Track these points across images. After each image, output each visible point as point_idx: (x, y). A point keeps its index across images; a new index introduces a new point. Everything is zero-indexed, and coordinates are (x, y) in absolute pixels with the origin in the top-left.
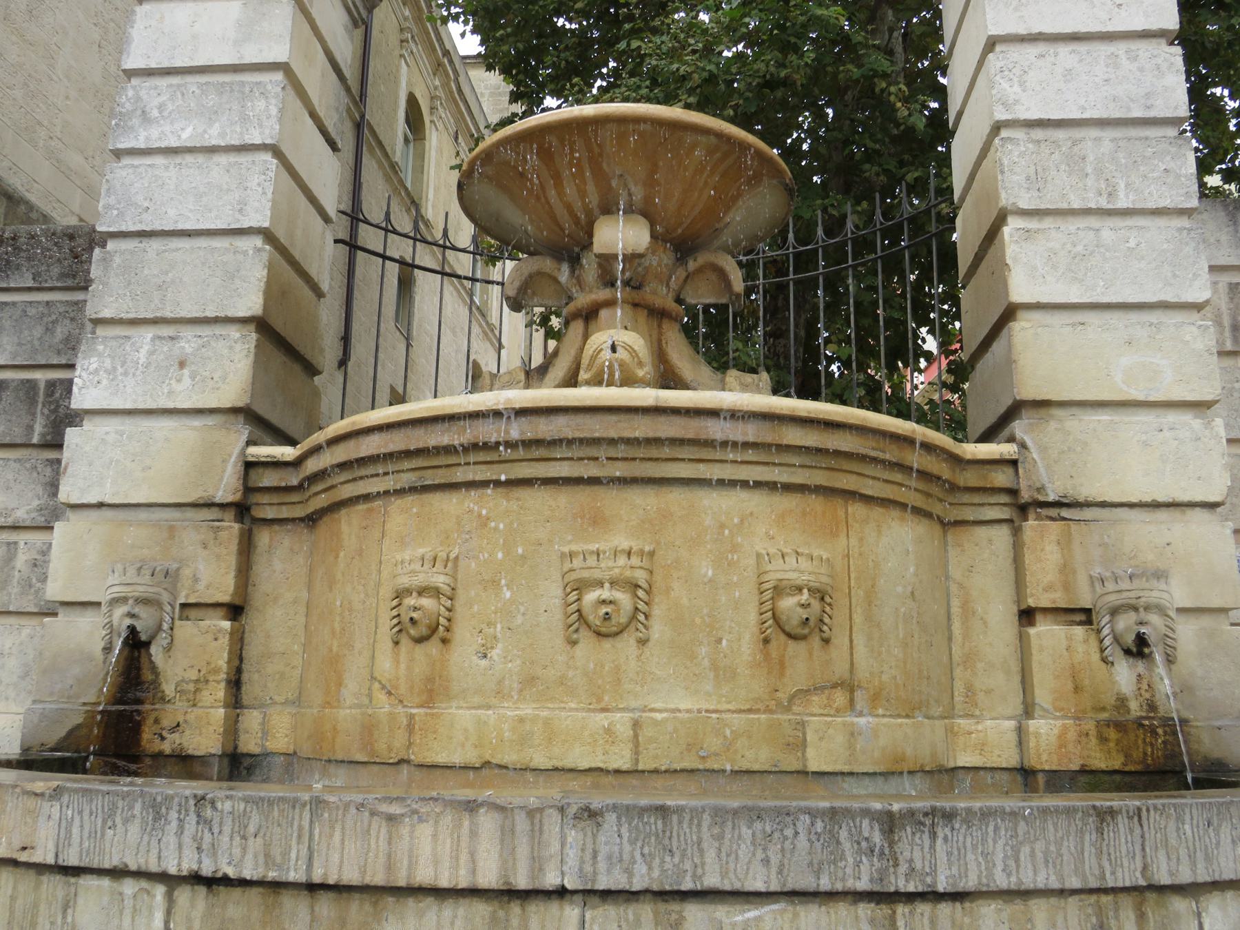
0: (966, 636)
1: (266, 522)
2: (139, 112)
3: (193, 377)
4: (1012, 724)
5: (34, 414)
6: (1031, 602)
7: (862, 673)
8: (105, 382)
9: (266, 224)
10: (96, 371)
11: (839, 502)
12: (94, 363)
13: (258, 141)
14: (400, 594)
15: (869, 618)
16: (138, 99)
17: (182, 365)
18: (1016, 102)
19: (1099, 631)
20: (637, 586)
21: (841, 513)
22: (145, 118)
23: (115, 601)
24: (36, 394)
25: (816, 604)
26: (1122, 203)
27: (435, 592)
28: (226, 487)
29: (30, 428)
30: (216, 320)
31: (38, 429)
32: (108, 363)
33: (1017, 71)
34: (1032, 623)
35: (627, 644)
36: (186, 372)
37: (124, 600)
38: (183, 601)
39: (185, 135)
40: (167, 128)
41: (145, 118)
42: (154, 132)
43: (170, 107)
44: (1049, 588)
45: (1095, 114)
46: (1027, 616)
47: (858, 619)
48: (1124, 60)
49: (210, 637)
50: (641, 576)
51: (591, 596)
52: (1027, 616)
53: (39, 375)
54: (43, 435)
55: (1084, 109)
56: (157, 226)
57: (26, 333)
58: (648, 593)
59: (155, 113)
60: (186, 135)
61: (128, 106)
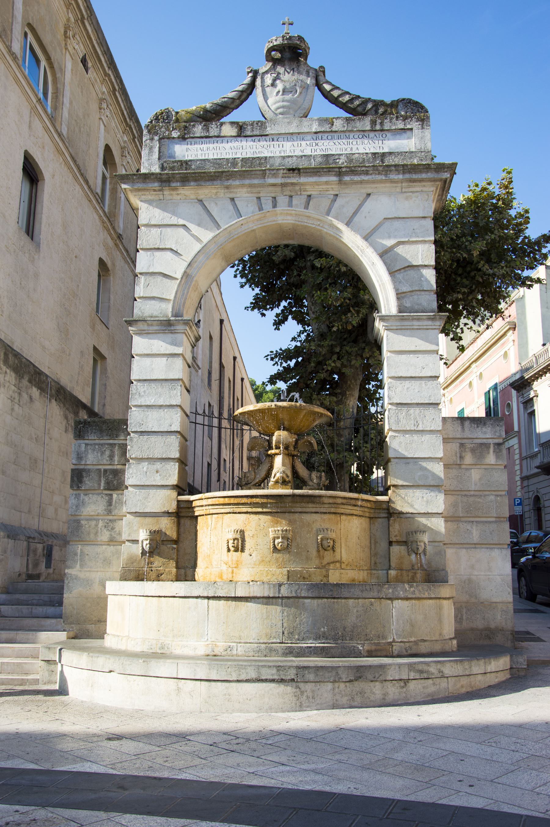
0: (375, 548)
1: (183, 517)
2: (138, 393)
4: (385, 572)
5: (100, 480)
6: (391, 540)
7: (344, 559)
8: (134, 477)
9: (179, 430)
10: (132, 474)
11: (339, 516)
13: (175, 404)
15: (346, 545)
17: (157, 472)
18: (393, 397)
19: (408, 547)
20: (288, 538)
21: (339, 518)
24: (101, 474)
25: (332, 542)
26: (420, 428)
28: (172, 507)
29: (100, 485)
30: (166, 459)
31: (102, 484)
32: (135, 470)
33: (394, 388)
34: (392, 545)
36: (158, 474)
38: (162, 539)
39: (152, 401)
40: (147, 399)
42: (143, 400)
43: (147, 392)
44: (396, 536)
45: (415, 402)
47: (343, 545)
48: (424, 385)
49: (171, 549)
50: (290, 536)
52: (391, 543)
53: (100, 467)
54: (104, 487)
55: (411, 400)
56: (147, 430)
57: (96, 454)
58: (292, 541)
59: (143, 393)
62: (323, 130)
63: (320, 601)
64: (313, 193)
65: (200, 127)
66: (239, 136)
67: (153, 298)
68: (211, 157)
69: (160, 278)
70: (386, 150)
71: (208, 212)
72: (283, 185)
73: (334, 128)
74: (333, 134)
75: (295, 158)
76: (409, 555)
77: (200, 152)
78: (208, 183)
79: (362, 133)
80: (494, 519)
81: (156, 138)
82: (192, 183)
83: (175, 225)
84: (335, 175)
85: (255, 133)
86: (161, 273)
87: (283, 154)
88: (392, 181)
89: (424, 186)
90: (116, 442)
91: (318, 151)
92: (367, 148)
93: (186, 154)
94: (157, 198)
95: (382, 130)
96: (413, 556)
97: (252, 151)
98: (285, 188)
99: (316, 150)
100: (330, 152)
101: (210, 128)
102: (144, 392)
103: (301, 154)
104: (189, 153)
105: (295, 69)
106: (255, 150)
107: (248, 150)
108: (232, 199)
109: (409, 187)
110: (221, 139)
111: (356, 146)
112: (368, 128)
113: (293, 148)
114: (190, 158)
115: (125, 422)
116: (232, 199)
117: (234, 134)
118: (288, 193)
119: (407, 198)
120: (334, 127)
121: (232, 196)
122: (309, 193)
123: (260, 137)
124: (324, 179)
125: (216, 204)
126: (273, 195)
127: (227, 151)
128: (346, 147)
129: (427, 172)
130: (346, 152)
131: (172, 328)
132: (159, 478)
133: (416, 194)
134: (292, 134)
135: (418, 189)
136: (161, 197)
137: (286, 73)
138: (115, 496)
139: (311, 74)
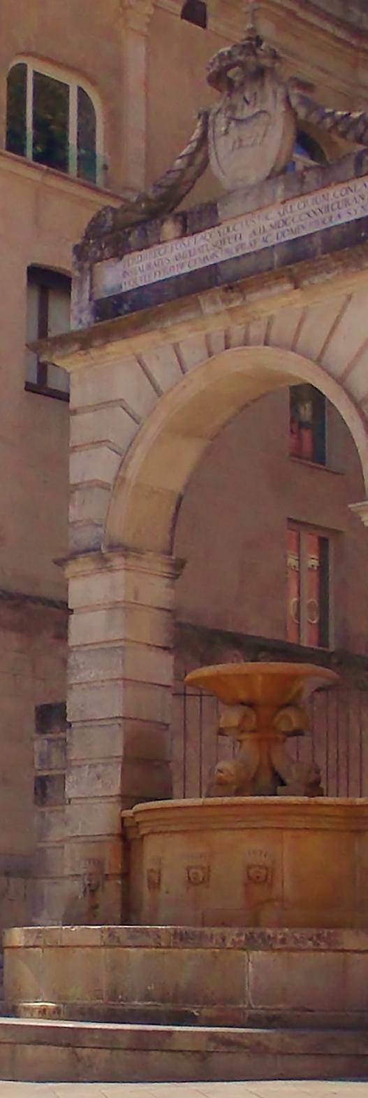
17: (99, 778)
36: (101, 780)
39: (92, 675)
65: (136, 233)
66: (184, 234)
68: (154, 280)
75: (253, 257)
79: (346, 185)
81: (87, 265)
91: (286, 233)
92: (352, 212)
97: (202, 256)
99: (283, 235)
101: (148, 233)
103: (264, 245)
105: (258, 94)
106: (206, 253)
108: (176, 347)
111: (337, 212)
112: (352, 173)
114: (129, 288)
115: (63, 706)
120: (305, 187)
123: (212, 229)
128: (321, 216)
130: (324, 227)
132: (100, 786)
137: (246, 105)
139: (278, 95)
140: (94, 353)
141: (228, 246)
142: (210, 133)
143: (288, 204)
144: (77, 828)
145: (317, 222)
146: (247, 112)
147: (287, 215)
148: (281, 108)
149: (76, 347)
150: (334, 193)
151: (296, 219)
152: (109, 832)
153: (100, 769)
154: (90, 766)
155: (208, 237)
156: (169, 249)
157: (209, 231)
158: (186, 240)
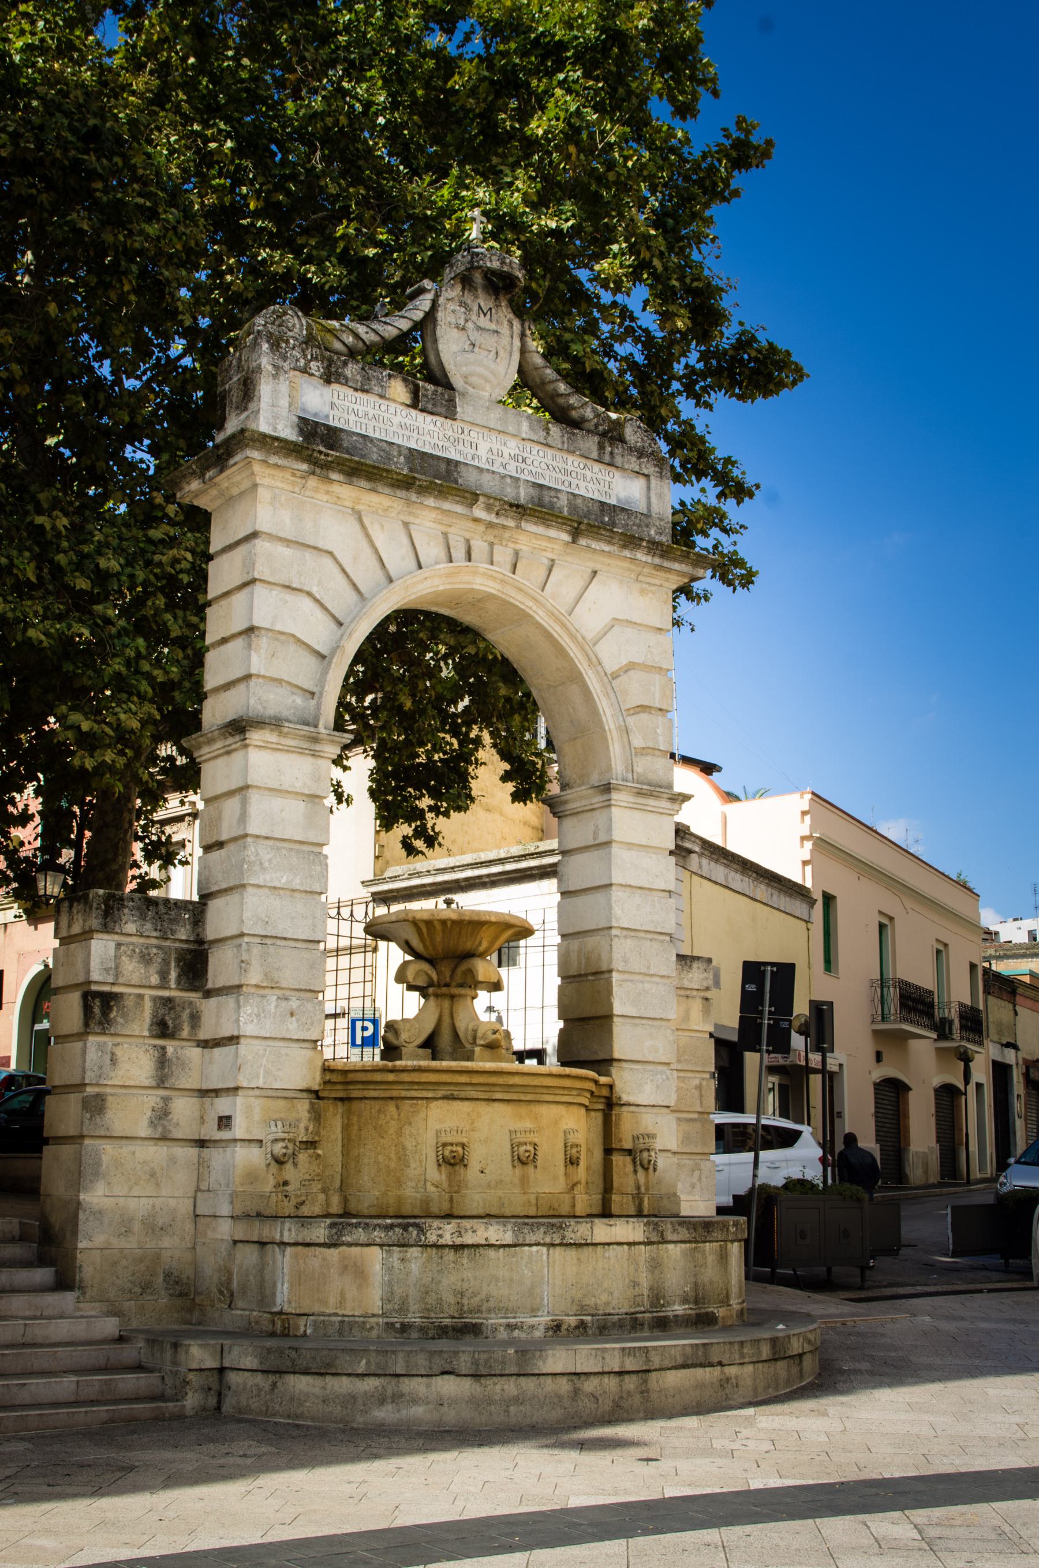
3: (298, 1021)
12: (248, 1010)
14: (444, 1145)
16: (257, 854)
17: (292, 1014)
22: (263, 869)
23: (276, 1140)
27: (463, 1146)
35: (530, 1169)
37: (283, 1140)
39: (284, 880)
41: (263, 869)
42: (268, 877)
46: (608, 1151)
51: (523, 1148)
60: (283, 879)
61: (252, 858)
62: (535, 438)
63: (683, 1245)
64: (523, 548)
67: (279, 681)
69: (292, 647)
70: (613, 501)
71: (368, 536)
72: (490, 525)
73: (550, 441)
74: (547, 449)
76: (635, 1172)
77: (352, 418)
78: (387, 490)
79: (584, 461)
80: (696, 1116)
82: (363, 483)
83: (315, 548)
84: (567, 532)
85: (439, 409)
86: (293, 636)
87: (476, 463)
88: (633, 560)
89: (667, 580)
90: (168, 943)
93: (331, 413)
94: (290, 488)
95: (610, 464)
96: (641, 1172)
98: (490, 531)
100: (541, 482)
102: (270, 861)
104: (335, 412)
107: (427, 438)
109: (650, 575)
110: (386, 402)
112: (595, 455)
113: (490, 455)
116: (406, 525)
117: (408, 402)
118: (491, 538)
119: (642, 592)
121: (406, 519)
122: (518, 547)
124: (553, 533)
125: (382, 527)
126: (468, 535)
127: (394, 428)
128: (564, 478)
129: (681, 562)
131: (318, 747)
133: (653, 588)
134: (490, 429)
135: (658, 582)
136: (297, 490)
138: (170, 1050)
140: (313, 482)
141: (461, 447)
142: (440, 315)
143: (528, 444)
144: (257, 1076)
145: (557, 480)
146: (484, 322)
147: (525, 455)
148: (517, 343)
149: (305, 467)
150: (574, 462)
151: (536, 463)
152: (303, 1085)
153: (294, 1004)
154: (279, 998)
155: (438, 424)
156: (392, 410)
157: (442, 419)
158: (414, 412)
